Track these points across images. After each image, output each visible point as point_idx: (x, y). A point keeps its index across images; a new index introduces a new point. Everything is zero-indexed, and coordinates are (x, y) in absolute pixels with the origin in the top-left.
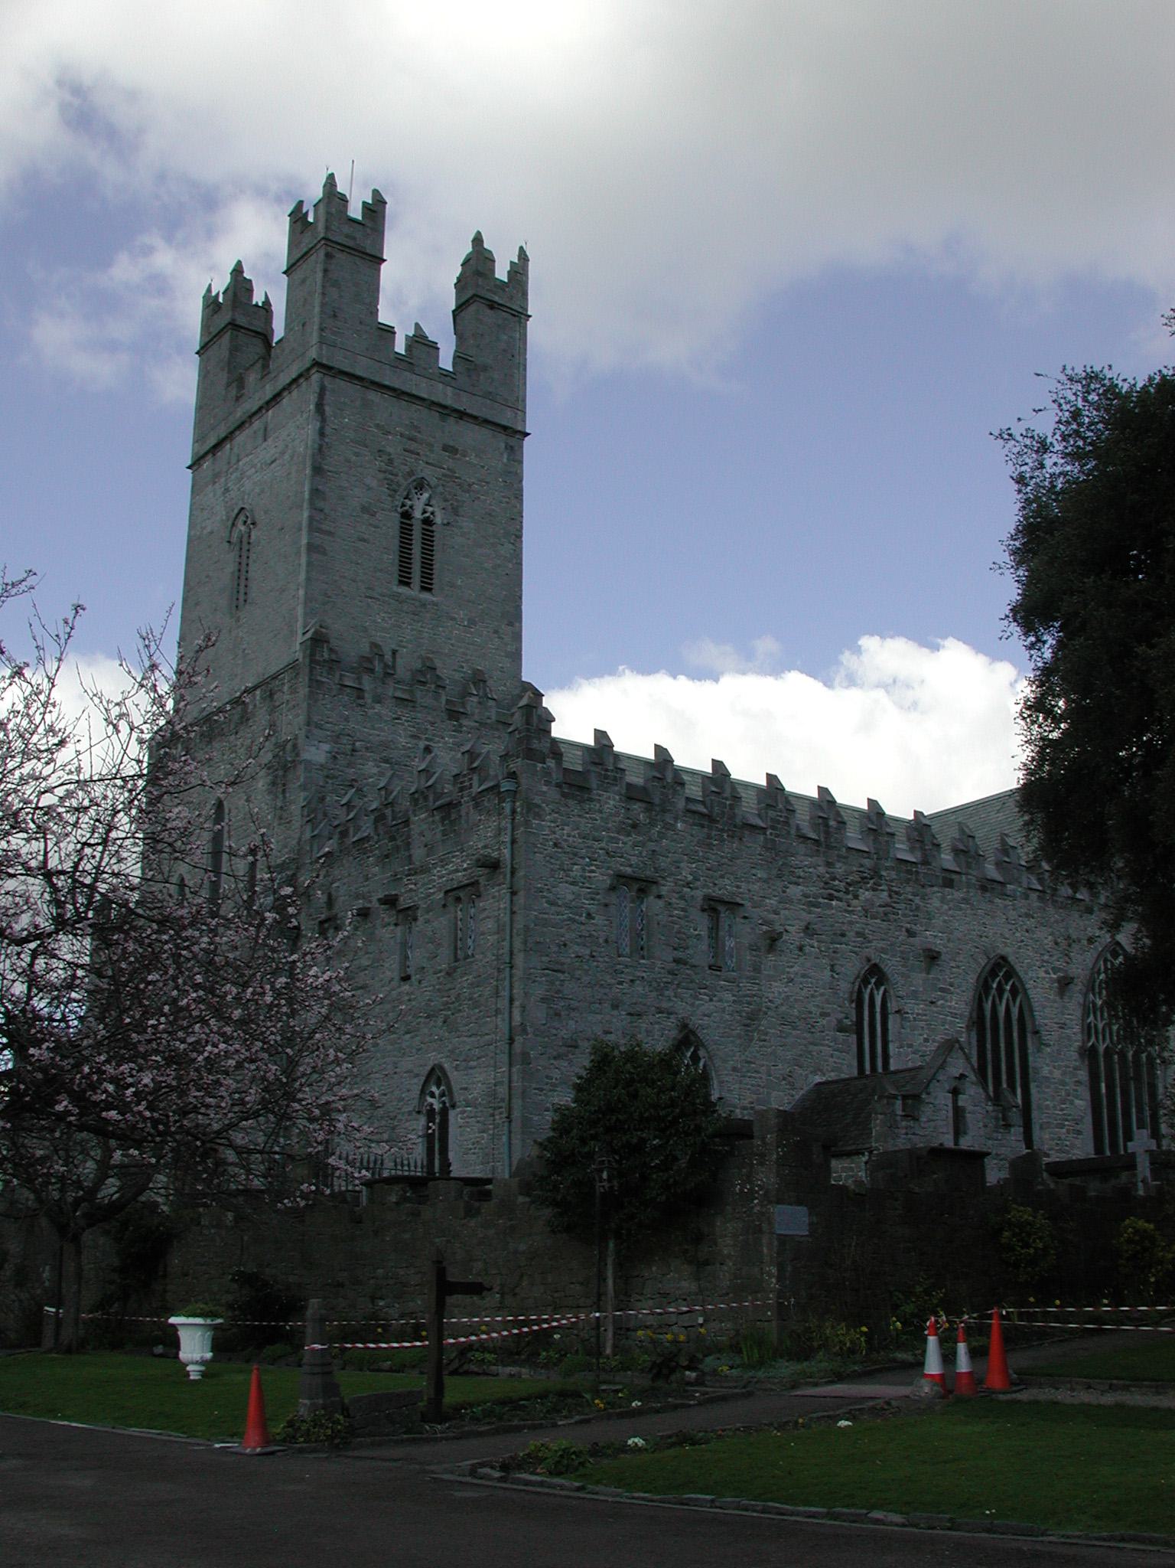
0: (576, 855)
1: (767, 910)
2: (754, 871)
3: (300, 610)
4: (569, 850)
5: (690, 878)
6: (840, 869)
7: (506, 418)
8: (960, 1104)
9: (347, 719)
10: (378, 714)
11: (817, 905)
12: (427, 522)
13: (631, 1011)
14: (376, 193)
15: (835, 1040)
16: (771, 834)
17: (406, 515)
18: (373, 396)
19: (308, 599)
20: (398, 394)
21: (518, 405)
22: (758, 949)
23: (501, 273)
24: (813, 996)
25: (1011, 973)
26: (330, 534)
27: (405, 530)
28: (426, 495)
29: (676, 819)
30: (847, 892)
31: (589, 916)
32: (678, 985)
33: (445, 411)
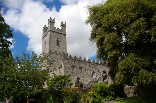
7: (65, 34)
25: (105, 71)
27: (57, 42)
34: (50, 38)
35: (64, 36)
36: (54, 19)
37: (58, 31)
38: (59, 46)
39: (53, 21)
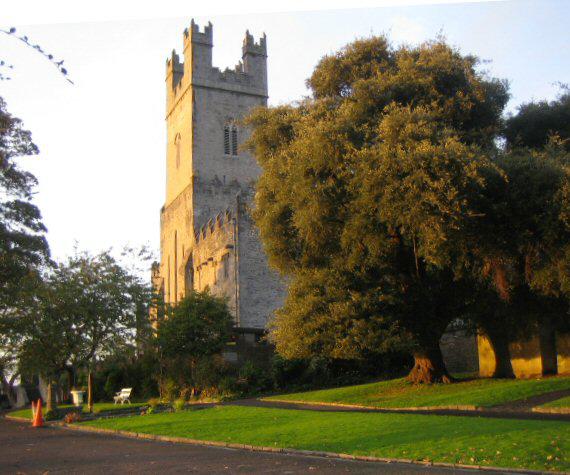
7: (260, 93)
12: (234, 132)
17: (226, 131)
18: (213, 93)
20: (221, 90)
21: (265, 87)
33: (239, 94)
36: (211, 25)
37: (226, 86)
38: (235, 153)
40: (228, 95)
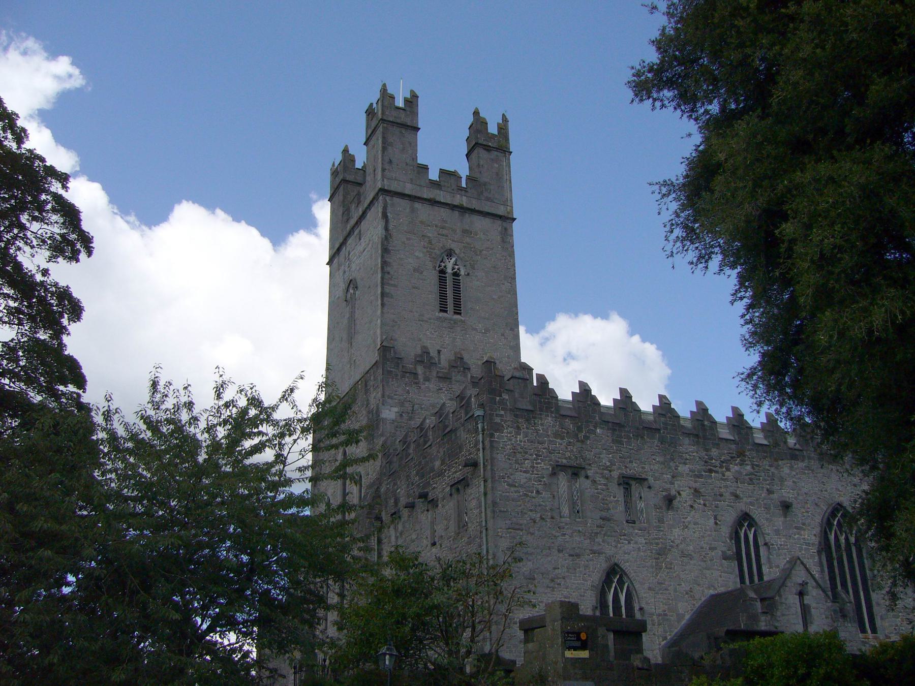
0: (526, 453)
1: (666, 482)
2: (654, 457)
3: (379, 332)
4: (521, 450)
5: (608, 464)
6: (714, 452)
7: (501, 211)
8: (805, 602)
9: (408, 392)
10: (428, 388)
11: (700, 476)
12: (456, 274)
13: (572, 553)
14: (412, 91)
15: (721, 565)
16: (664, 433)
17: (443, 272)
18: (417, 205)
19: (383, 324)
20: (433, 202)
21: (507, 203)
22: (661, 508)
23: (493, 129)
24: (703, 537)
26: (395, 286)
27: (442, 280)
28: (454, 259)
29: (595, 427)
30: (721, 467)
31: (538, 492)
32: (605, 535)
33: (463, 210)
34: (385, 250)
35: (492, 228)
38: (458, 312)
39: (403, 118)
40: (444, 213)
